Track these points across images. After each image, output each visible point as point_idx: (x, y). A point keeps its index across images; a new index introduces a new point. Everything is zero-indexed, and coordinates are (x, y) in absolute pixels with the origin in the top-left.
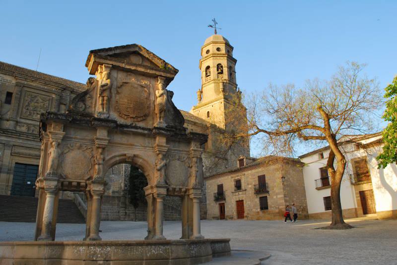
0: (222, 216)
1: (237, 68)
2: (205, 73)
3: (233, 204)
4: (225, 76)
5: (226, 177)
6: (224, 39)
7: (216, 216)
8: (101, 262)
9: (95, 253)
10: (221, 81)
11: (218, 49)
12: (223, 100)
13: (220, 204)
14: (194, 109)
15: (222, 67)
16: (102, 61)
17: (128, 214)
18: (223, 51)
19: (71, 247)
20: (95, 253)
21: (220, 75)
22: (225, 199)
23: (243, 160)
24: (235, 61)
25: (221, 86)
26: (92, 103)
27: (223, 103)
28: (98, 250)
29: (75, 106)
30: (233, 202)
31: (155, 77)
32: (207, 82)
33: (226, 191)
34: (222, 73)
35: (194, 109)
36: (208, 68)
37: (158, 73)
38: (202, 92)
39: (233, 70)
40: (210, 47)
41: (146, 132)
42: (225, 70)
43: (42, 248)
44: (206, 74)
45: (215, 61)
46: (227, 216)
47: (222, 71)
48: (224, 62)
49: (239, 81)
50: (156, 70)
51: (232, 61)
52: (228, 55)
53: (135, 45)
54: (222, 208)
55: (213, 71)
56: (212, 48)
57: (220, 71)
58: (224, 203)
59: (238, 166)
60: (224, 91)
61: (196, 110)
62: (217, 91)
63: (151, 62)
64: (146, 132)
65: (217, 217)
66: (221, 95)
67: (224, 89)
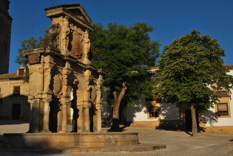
23: (23, 69)
59: (18, 74)
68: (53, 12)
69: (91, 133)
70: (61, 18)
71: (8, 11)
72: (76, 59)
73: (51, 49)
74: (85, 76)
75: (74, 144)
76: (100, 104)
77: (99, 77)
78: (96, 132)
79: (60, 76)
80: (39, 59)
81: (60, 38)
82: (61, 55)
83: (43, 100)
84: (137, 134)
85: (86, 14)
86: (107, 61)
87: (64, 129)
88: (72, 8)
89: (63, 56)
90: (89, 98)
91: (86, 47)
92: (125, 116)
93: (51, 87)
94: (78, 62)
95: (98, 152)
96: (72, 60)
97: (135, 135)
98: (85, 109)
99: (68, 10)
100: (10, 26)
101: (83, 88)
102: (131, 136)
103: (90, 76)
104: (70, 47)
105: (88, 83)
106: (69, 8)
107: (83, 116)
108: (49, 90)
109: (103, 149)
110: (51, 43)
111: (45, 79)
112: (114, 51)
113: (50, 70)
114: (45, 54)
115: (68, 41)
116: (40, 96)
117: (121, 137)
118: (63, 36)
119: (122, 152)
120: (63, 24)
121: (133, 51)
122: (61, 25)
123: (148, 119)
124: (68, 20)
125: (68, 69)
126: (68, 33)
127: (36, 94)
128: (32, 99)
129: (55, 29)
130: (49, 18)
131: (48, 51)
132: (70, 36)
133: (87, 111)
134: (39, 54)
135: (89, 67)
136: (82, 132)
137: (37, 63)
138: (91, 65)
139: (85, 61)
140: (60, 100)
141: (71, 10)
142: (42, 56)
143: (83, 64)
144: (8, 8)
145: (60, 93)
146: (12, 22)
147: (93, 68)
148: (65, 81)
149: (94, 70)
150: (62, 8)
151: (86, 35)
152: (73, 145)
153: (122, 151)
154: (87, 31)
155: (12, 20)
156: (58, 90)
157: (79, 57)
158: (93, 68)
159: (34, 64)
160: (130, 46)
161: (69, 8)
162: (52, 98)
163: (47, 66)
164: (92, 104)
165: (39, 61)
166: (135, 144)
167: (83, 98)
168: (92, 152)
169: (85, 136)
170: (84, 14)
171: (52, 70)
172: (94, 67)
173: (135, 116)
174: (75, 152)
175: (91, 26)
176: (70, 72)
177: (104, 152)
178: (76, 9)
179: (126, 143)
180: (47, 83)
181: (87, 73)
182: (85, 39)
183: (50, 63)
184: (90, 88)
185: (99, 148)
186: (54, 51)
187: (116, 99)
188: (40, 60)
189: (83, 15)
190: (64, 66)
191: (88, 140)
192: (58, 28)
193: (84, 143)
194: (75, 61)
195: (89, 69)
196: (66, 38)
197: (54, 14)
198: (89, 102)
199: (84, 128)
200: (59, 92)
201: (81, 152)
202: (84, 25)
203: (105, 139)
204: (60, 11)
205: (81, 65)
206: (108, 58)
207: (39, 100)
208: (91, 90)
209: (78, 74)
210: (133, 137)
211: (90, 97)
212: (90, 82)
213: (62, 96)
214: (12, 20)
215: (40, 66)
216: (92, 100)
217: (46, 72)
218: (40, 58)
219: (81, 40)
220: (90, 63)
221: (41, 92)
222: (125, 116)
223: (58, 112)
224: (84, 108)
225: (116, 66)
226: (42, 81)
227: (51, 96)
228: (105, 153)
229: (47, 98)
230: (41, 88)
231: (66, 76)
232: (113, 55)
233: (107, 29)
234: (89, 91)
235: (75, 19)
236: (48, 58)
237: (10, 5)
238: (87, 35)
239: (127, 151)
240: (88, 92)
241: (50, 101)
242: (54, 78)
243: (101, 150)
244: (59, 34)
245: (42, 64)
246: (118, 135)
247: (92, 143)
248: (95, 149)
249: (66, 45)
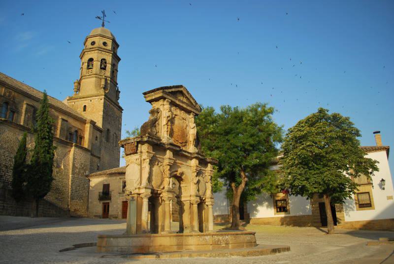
0: (106, 213)
1: (120, 66)
2: (87, 64)
3: (118, 204)
4: (108, 73)
5: (114, 178)
6: (112, 35)
7: (98, 215)
8: (224, 245)
9: (219, 240)
10: (103, 77)
11: (105, 44)
12: (103, 96)
13: (104, 203)
14: (68, 100)
15: (106, 63)
16: (166, 96)
17: (6, 208)
18: (109, 47)
19: (195, 237)
20: (219, 240)
21: (103, 71)
22: (110, 199)
24: (119, 59)
25: (103, 82)
26: (159, 129)
27: (103, 101)
28: (221, 238)
29: (151, 131)
30: (119, 202)
31: (189, 112)
32: (87, 74)
33: (113, 191)
34: (104, 69)
35: (68, 100)
36: (91, 60)
37: (193, 110)
38: (79, 84)
39: (115, 68)
40: (96, 39)
41: (189, 155)
42: (109, 67)
43: (172, 238)
44: (88, 66)
45: (100, 55)
46: (111, 216)
47: (105, 66)
48: (109, 58)
49: (120, 80)
50: (192, 108)
51: (116, 58)
52: (114, 52)
53: (181, 86)
54: (106, 208)
55: (97, 65)
56: (99, 41)
57: (103, 66)
58: (109, 203)
60: (105, 88)
61: (72, 101)
62: (98, 85)
63: (188, 99)
64: (189, 155)
65: (99, 216)
66: (102, 92)
67: (105, 86)
68: (152, 95)
69: (200, 233)
70: (161, 102)
71: (118, 101)
72: (179, 147)
73: (149, 137)
74: (191, 167)
75: (176, 247)
76: (211, 198)
77: (208, 166)
78: (207, 233)
79: (161, 167)
80: (135, 148)
81: (160, 123)
82: (161, 143)
83: (141, 196)
84: (254, 234)
85: (191, 96)
86: (221, 149)
87: (167, 229)
88: (173, 90)
89: (164, 144)
90: (197, 192)
91: (192, 132)
92: (150, 212)
93: (150, 179)
94: (181, 150)
95: (203, 257)
96: (174, 148)
97: (252, 236)
98: (192, 204)
99: (169, 92)
100: (120, 117)
101: (190, 181)
102: (245, 236)
103: (197, 166)
104: (171, 134)
105: (196, 173)
106: (170, 90)
107: (191, 213)
108: (147, 184)
109: (209, 254)
110: (150, 130)
111: (143, 172)
112: (230, 137)
113: (148, 160)
114: (142, 143)
115: (169, 127)
116: (137, 191)
117: (233, 237)
118: (163, 121)
119: (233, 257)
120: (164, 108)
121: (252, 135)
122: (162, 109)
123: (275, 214)
124: (168, 103)
125: (169, 159)
126: (169, 118)
127: (133, 188)
128: (129, 195)
129: (154, 114)
130: (148, 103)
131: (145, 139)
132: (171, 120)
133: (195, 207)
134: (136, 143)
135: (196, 155)
136: (190, 232)
137: (133, 153)
138: (198, 153)
139: (191, 148)
140: (161, 196)
141: (172, 93)
142: (139, 145)
143: (188, 153)
144: (118, 98)
145: (162, 187)
146: (122, 112)
147: (200, 156)
148: (168, 173)
149: (201, 159)
150: (161, 91)
151: (190, 120)
152: (175, 249)
153: (233, 255)
154: (193, 114)
155: (123, 110)
156: (159, 184)
157: (183, 144)
158: (200, 156)
159: (130, 154)
160: (248, 130)
161: (170, 90)
162: (151, 193)
163: (145, 156)
164: (201, 199)
165: (135, 150)
166: (251, 246)
167: (189, 193)
168: (196, 258)
169: (190, 238)
170: (187, 96)
171: (151, 161)
172: (201, 155)
173: (257, 211)
174: (176, 257)
175: (197, 110)
176: (172, 162)
177: (210, 257)
178: (179, 91)
179: (240, 245)
180: (145, 175)
181: (194, 162)
182: (190, 124)
183: (147, 152)
184: (197, 180)
185: (205, 252)
186: (152, 138)
187: (235, 192)
188: (137, 150)
189: (187, 97)
190: (165, 154)
191: (193, 242)
192: (158, 113)
193: (189, 246)
194: (178, 149)
195: (196, 158)
196: (167, 124)
197: (153, 98)
198: (197, 196)
199: (192, 227)
200: (160, 186)
201: (183, 258)
202: (189, 108)
203: (213, 242)
204: (159, 94)
205: (187, 154)
206: (223, 145)
207: (136, 195)
208: (198, 182)
209: (181, 164)
210: (248, 238)
211: (198, 190)
212: (197, 173)
213: (163, 190)
214: (123, 110)
215: (136, 156)
216: (201, 193)
217: (144, 163)
218: (137, 146)
219: (185, 126)
220: (197, 151)
221: (138, 186)
222: (150, 212)
223: (159, 207)
224: (191, 204)
225: (233, 154)
226: (139, 174)
227: (149, 191)
228: (211, 258)
229: (145, 194)
230: (138, 182)
231: (169, 167)
232: (228, 140)
233: (220, 113)
234: (196, 184)
235: (178, 102)
236: (145, 147)
237: (121, 95)
238: (193, 119)
239: (239, 255)
240: (195, 185)
241: (148, 196)
242: (153, 169)
243: (206, 254)
244: (159, 119)
245: (139, 154)
246: (229, 236)
247: (198, 246)
248: (200, 253)
249: (167, 131)
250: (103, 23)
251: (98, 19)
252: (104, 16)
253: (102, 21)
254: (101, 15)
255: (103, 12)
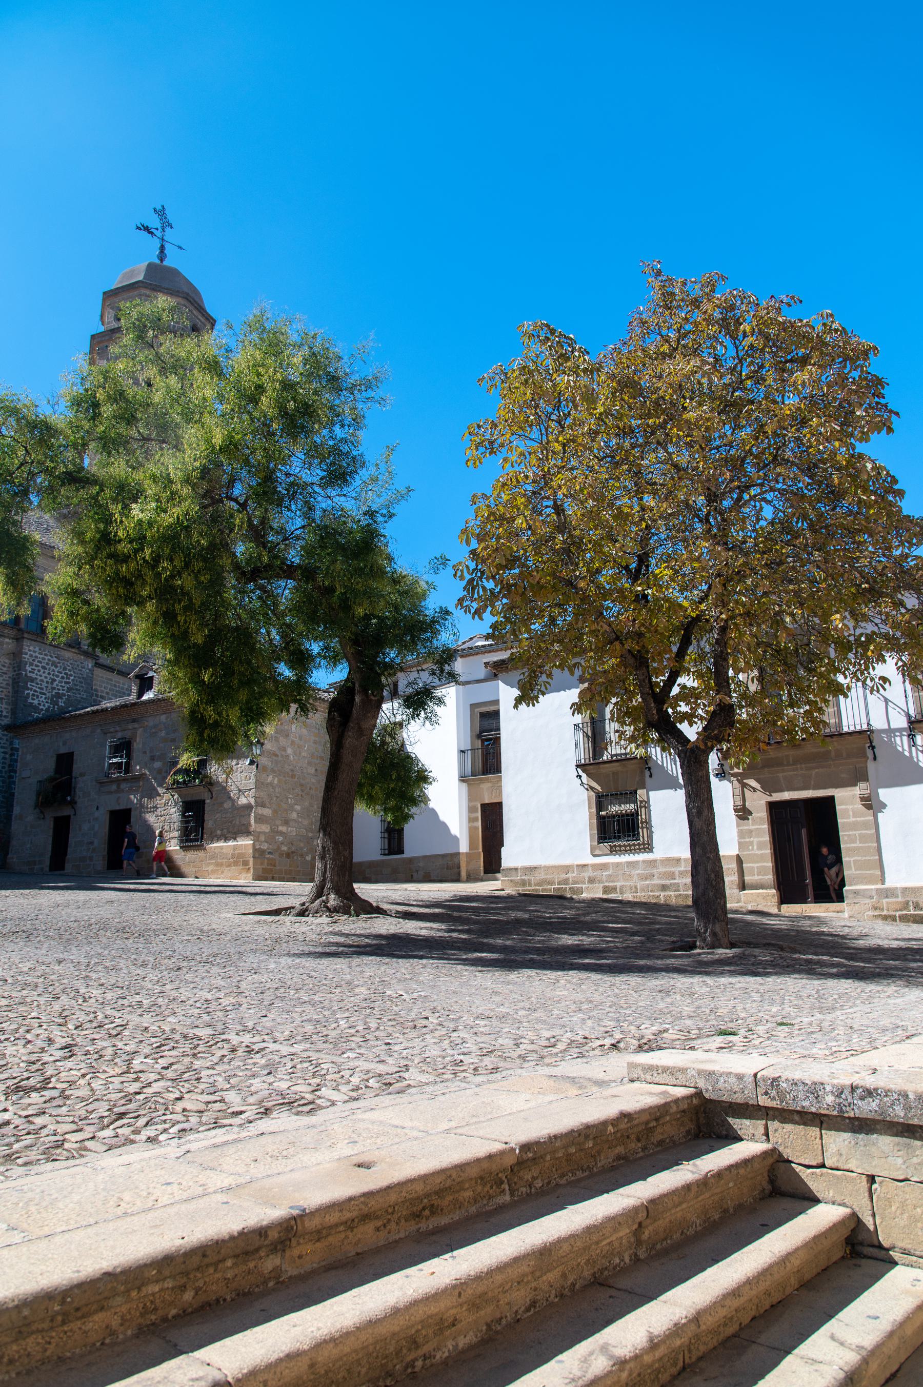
250: (162, 248)
251: (146, 233)
252: (166, 224)
253: (157, 243)
254: (154, 222)
255: (161, 213)
